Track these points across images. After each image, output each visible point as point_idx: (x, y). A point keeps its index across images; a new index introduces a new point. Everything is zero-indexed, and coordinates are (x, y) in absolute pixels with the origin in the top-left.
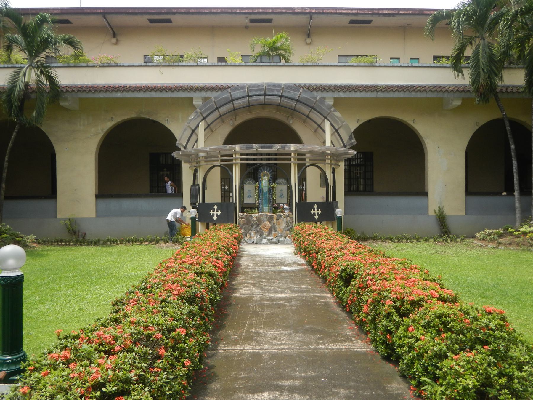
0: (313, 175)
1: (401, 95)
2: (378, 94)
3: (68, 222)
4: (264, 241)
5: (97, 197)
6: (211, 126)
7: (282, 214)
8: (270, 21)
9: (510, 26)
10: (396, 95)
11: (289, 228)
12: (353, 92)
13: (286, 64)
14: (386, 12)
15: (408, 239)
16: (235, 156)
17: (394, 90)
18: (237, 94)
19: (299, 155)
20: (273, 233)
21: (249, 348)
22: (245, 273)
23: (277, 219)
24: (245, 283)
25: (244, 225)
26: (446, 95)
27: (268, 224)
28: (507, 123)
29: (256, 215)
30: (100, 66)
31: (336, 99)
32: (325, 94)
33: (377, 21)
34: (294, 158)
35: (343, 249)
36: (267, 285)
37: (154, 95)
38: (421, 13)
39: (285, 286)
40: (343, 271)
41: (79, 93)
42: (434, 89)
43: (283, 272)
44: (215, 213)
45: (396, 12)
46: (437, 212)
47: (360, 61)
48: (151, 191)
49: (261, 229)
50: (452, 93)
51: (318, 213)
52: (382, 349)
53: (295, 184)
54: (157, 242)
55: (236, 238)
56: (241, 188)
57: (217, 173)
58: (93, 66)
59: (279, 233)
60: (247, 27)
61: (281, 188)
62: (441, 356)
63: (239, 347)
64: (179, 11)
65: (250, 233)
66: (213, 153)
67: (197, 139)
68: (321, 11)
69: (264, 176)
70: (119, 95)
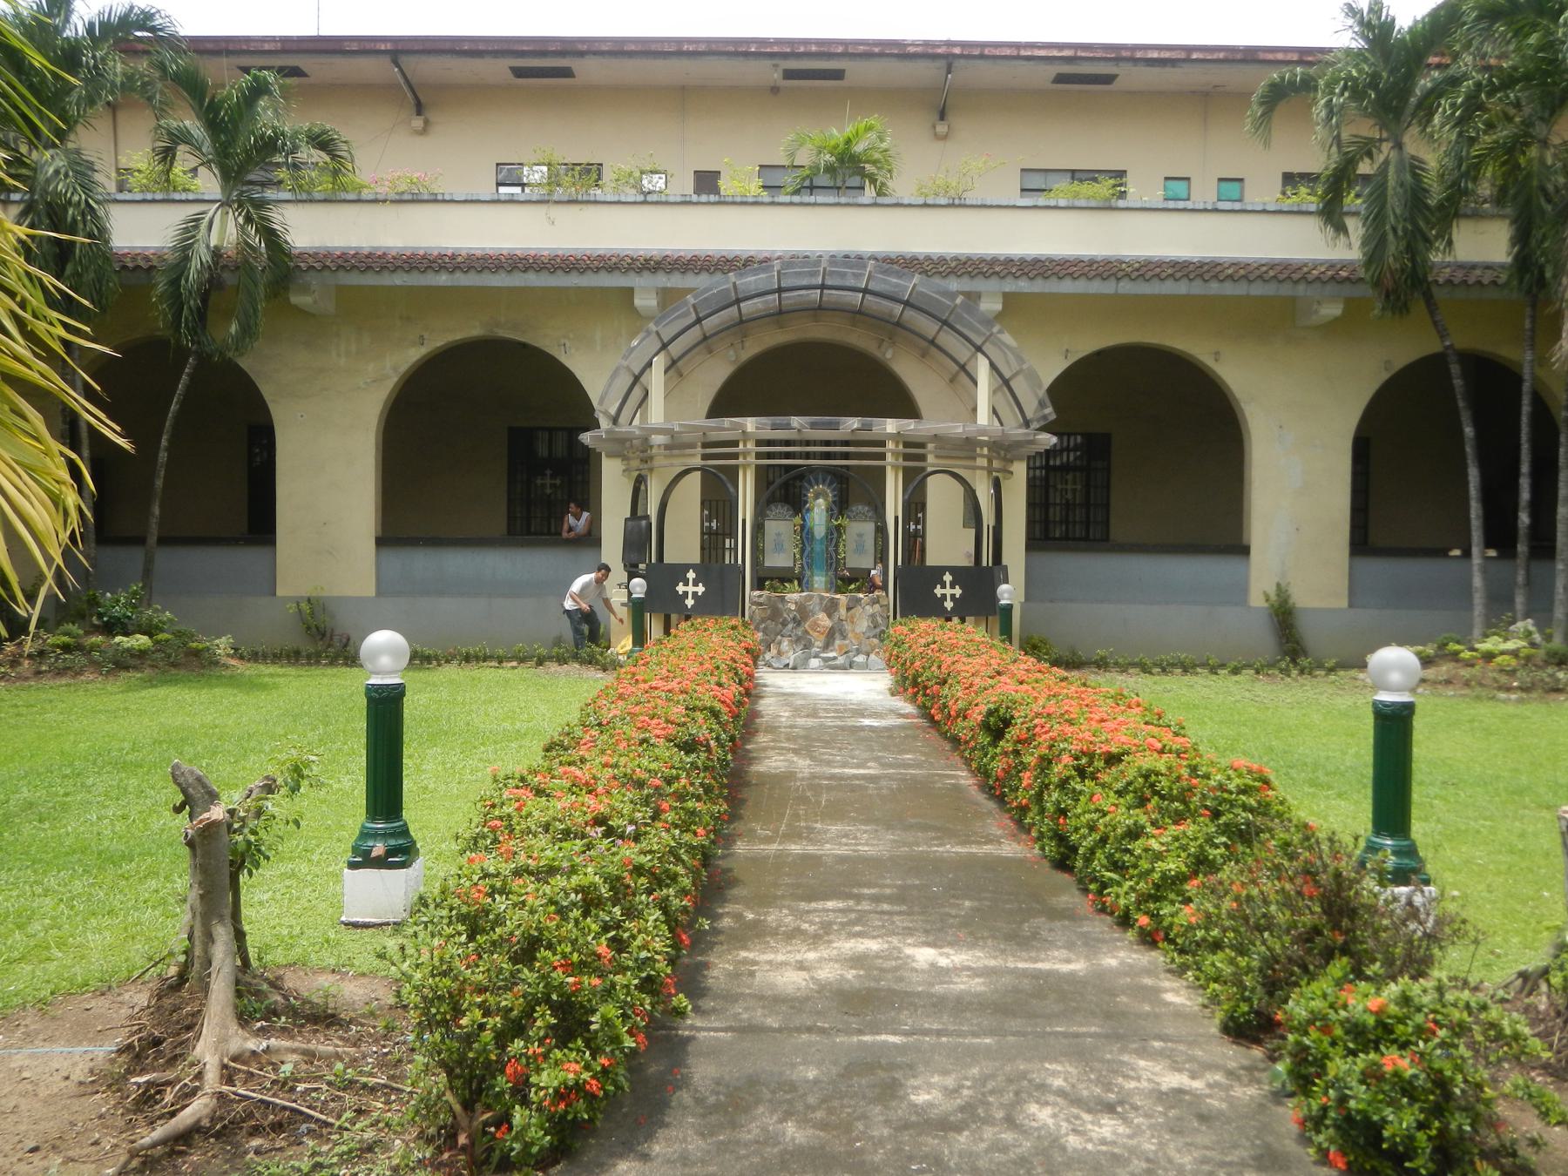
0: (942, 496)
1: (1182, 288)
2: (1122, 284)
3: (304, 606)
4: (814, 662)
5: (381, 542)
6: (680, 364)
8: (838, 75)
9: (1460, 122)
10: (1169, 288)
12: (1054, 279)
13: (880, 200)
14: (1155, 55)
15: (1187, 668)
17: (1164, 275)
18: (750, 281)
19: (907, 445)
20: (837, 642)
21: (795, 848)
22: (772, 729)
23: (849, 609)
24: (773, 748)
25: (763, 620)
26: (1301, 289)
27: (824, 621)
28: (1455, 369)
29: (795, 596)
30: (393, 202)
31: (1008, 298)
32: (978, 285)
33: (1130, 77)
34: (895, 454)
35: (999, 673)
36: (825, 753)
37: (533, 279)
38: (1250, 57)
39: (866, 755)
40: (990, 713)
41: (341, 274)
42: (1272, 273)
43: (862, 728)
44: (691, 589)
45: (1183, 55)
46: (1273, 597)
47: (1076, 195)
48: (511, 531)
49: (806, 632)
50: (1317, 285)
51: (953, 596)
52: (1051, 847)
54: (540, 663)
55: (748, 650)
56: (758, 528)
57: (691, 490)
58: (375, 201)
59: (851, 642)
60: (775, 90)
61: (859, 530)
62: (1135, 833)
63: (775, 846)
64: (596, 47)
65: (780, 643)
66: (687, 438)
67: (645, 400)
68: (976, 52)
69: (817, 497)
70: (443, 279)
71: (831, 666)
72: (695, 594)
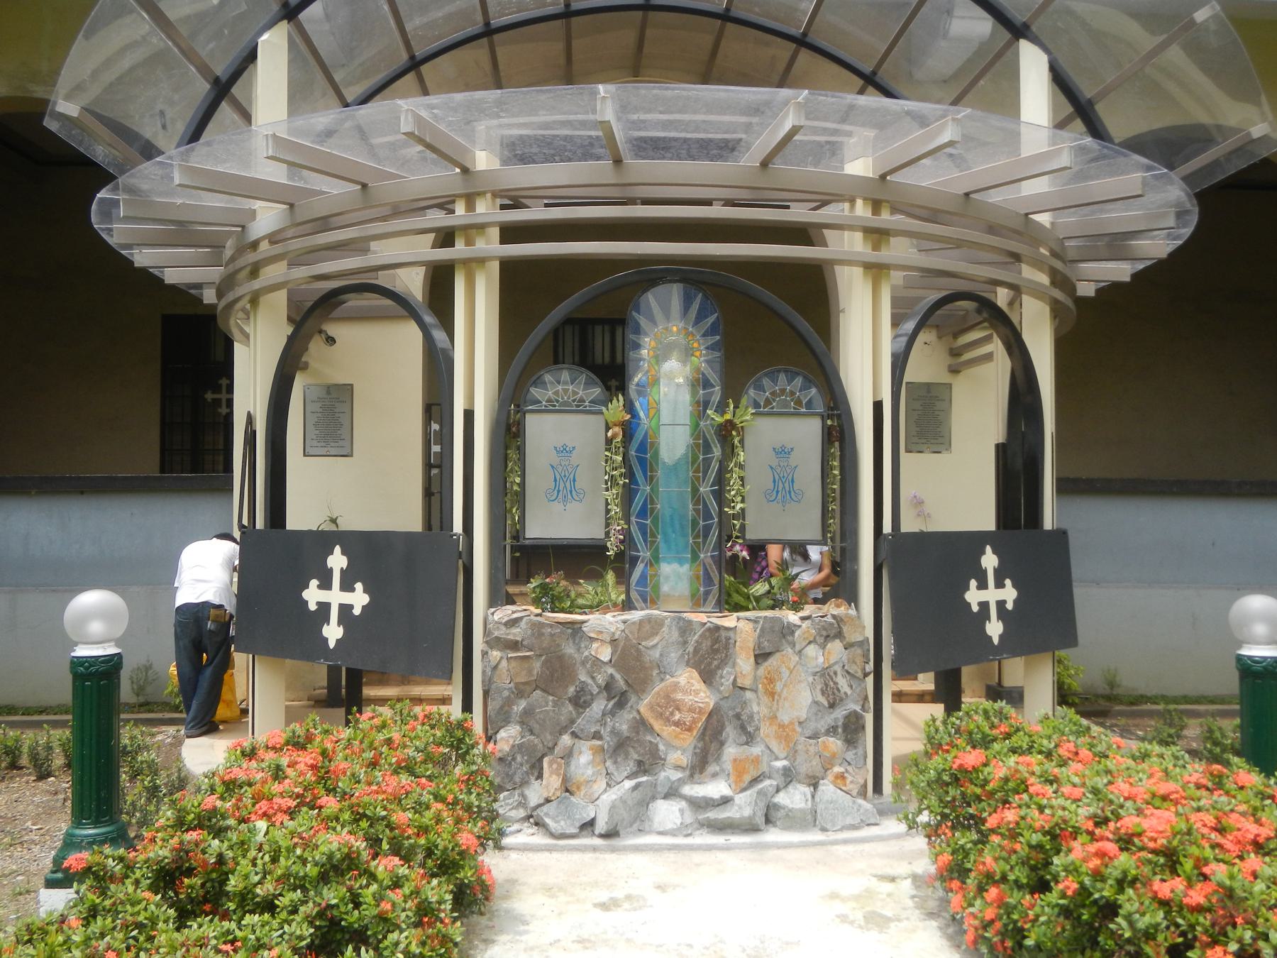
4: (667, 813)
7: (792, 617)
11: (840, 714)
16: (470, 207)
20: (731, 751)
23: (761, 657)
25: (520, 692)
27: (692, 690)
49: (641, 724)
53: (878, 406)
56: (509, 434)
61: (780, 439)
65: (568, 755)
69: (660, 358)
71: (712, 819)
72: (345, 609)
